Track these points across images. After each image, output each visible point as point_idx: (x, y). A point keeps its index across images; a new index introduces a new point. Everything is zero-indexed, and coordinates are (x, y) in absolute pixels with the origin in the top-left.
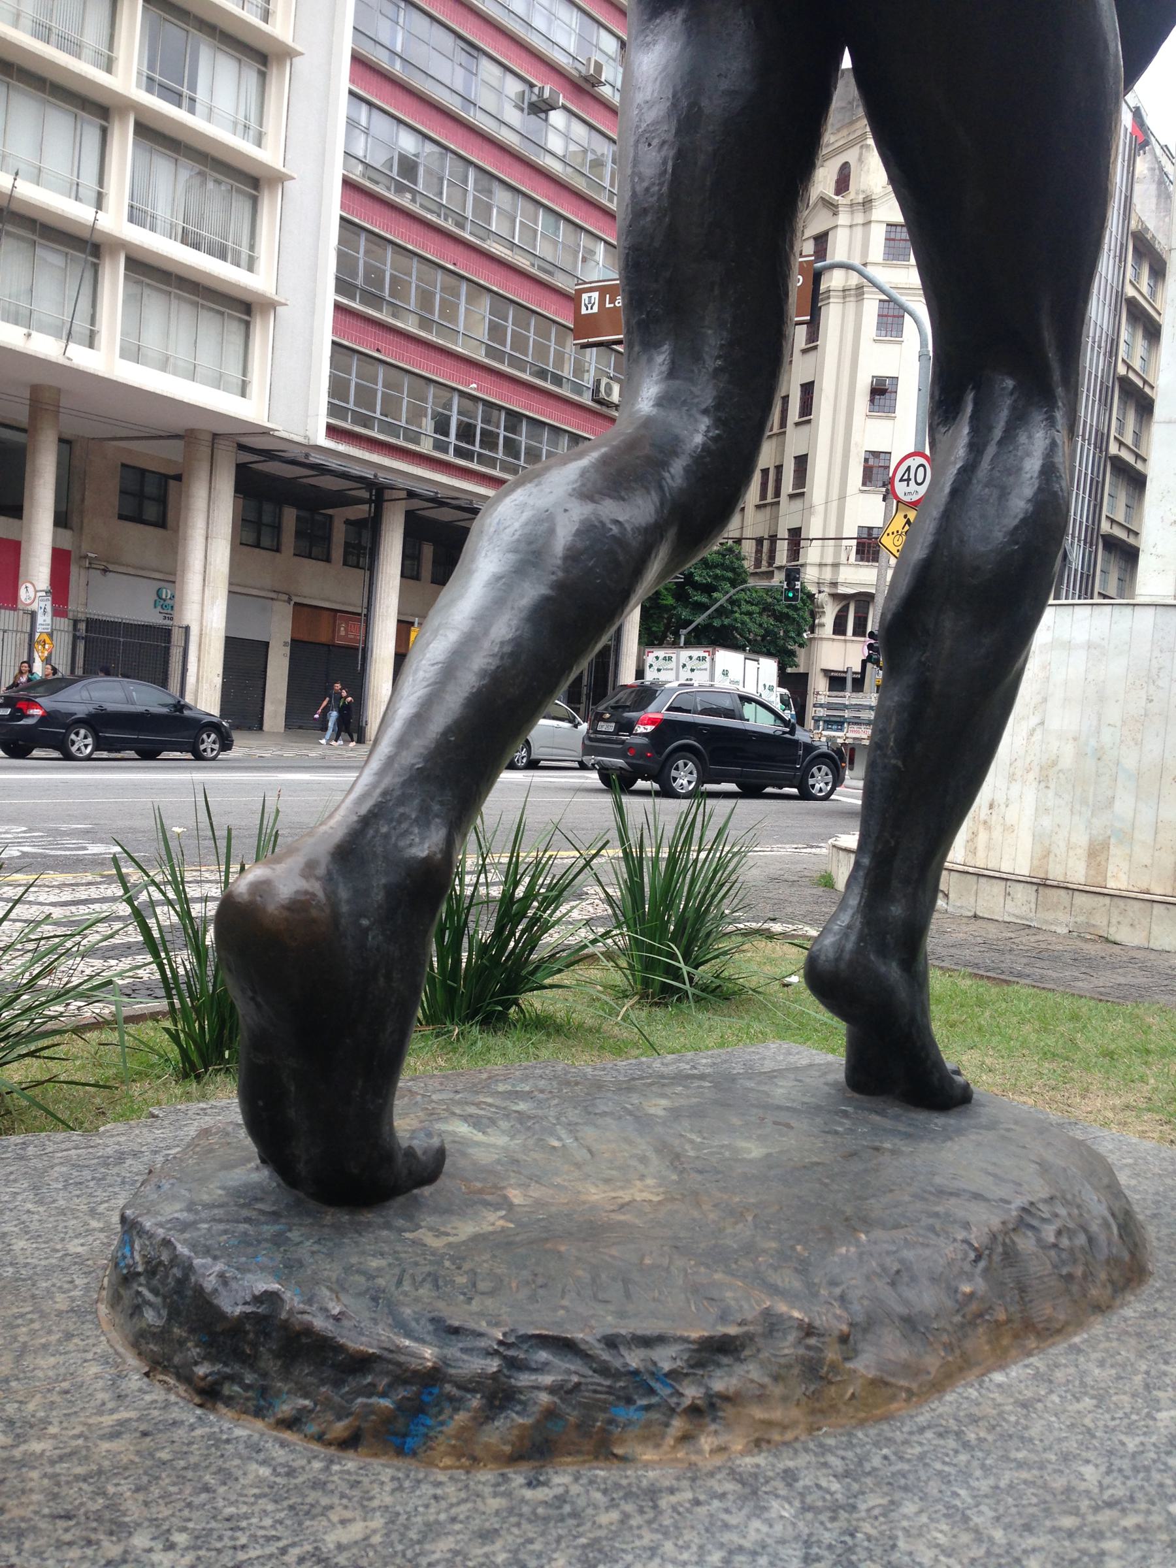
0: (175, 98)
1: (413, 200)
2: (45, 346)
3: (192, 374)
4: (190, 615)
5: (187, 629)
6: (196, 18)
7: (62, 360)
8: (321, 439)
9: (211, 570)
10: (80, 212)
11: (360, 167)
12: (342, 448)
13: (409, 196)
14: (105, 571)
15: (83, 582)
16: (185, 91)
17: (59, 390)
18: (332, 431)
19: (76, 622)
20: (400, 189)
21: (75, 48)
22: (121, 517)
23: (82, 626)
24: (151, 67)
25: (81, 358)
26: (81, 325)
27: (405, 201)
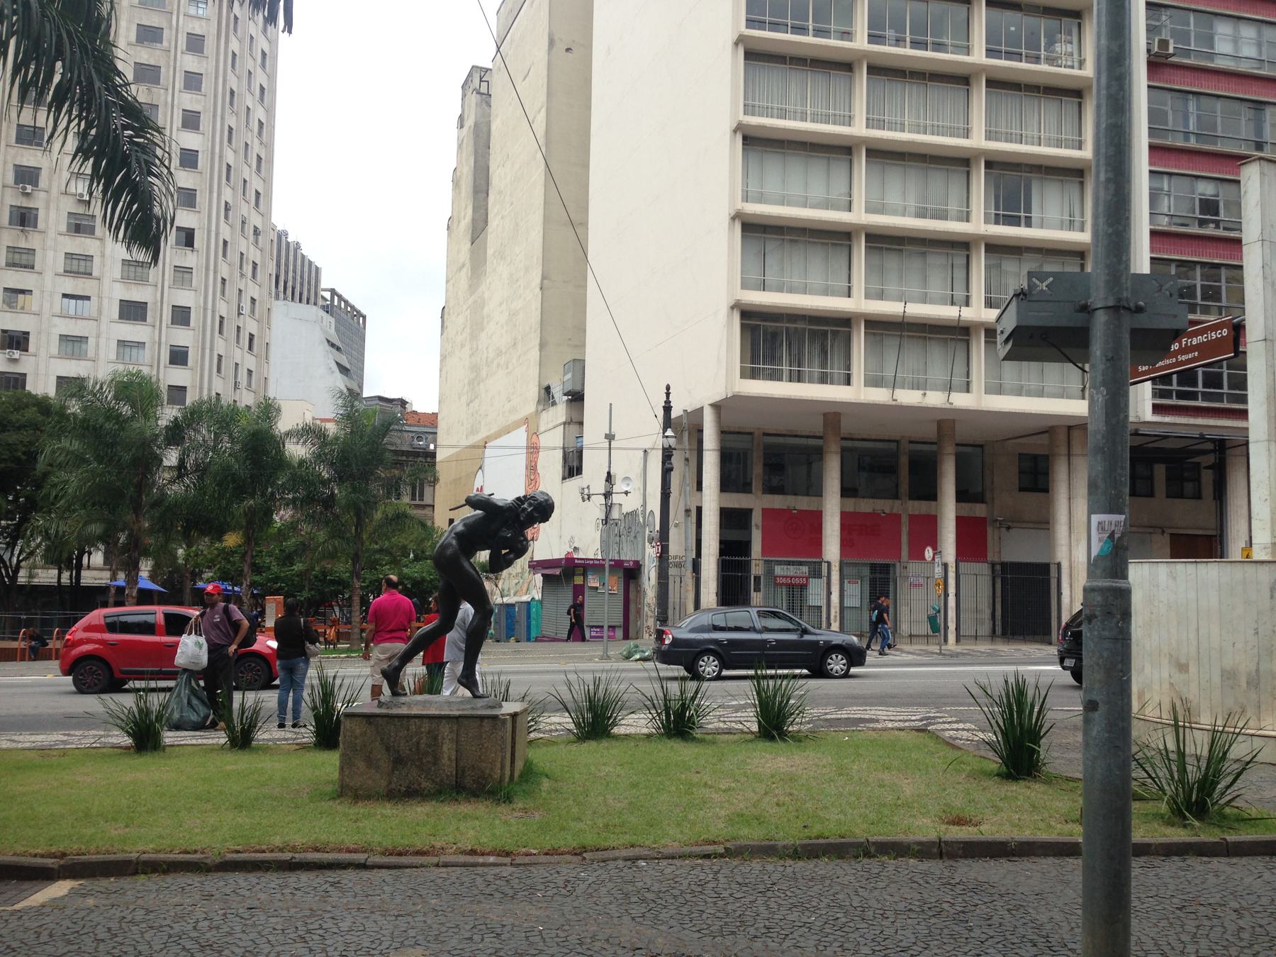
0: (1015, 221)
1: (1217, 227)
2: (935, 399)
3: (1041, 393)
4: (1061, 555)
5: (1059, 565)
6: (1027, 165)
7: (948, 406)
8: (1148, 416)
9: (1075, 520)
10: (947, 312)
11: (1166, 219)
12: (1167, 419)
13: (1212, 225)
14: (1008, 528)
15: (996, 538)
16: (1022, 214)
17: (954, 421)
18: (1157, 409)
19: (993, 565)
20: (1202, 223)
21: (943, 216)
22: (1021, 489)
23: (998, 567)
24: (997, 208)
25: (961, 401)
26: (958, 379)
27: (1210, 231)
